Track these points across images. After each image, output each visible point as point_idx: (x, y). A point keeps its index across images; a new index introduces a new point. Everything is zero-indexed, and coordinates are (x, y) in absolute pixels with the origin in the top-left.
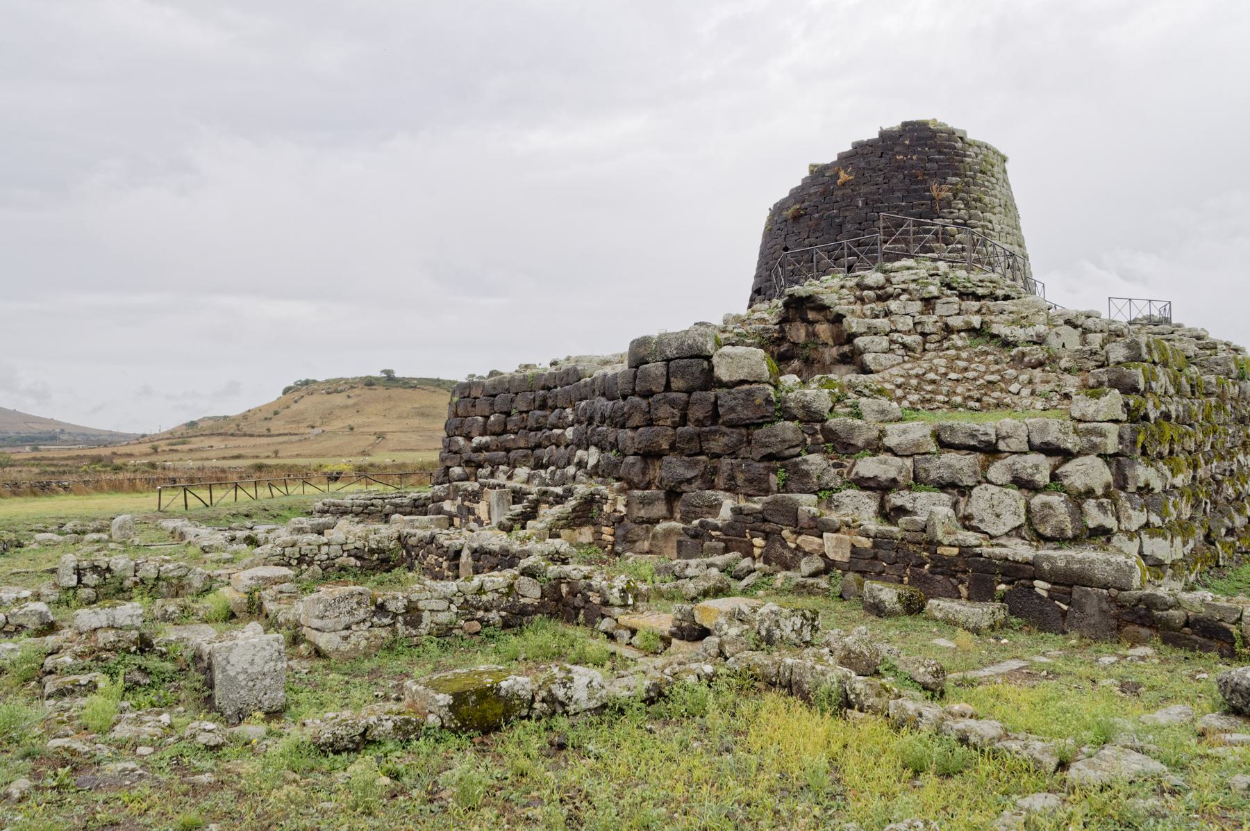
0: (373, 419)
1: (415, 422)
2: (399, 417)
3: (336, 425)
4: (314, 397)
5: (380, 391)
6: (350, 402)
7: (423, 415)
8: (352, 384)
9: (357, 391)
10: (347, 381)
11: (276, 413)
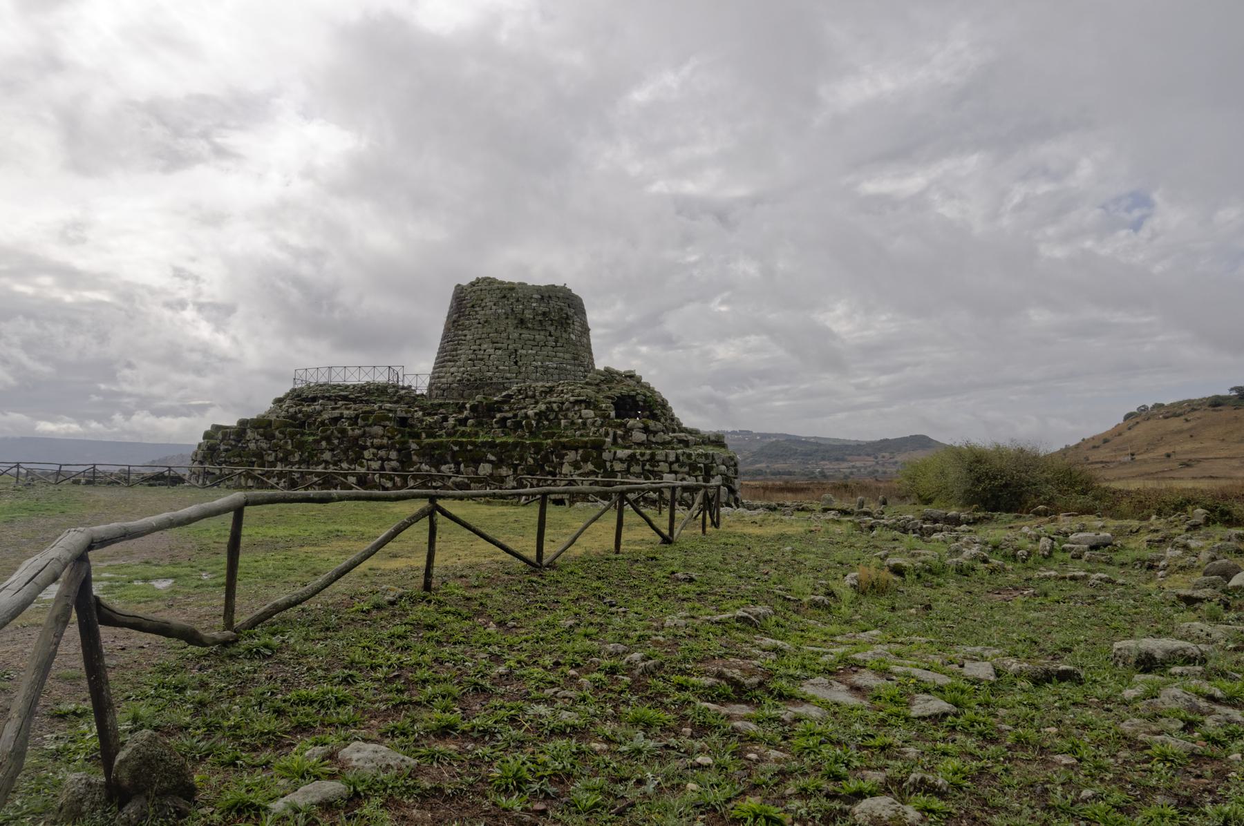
0: (1208, 444)
4: (1148, 423)
5: (1226, 412)
8: (1192, 406)
9: (1197, 414)
10: (1190, 402)
11: (1106, 441)
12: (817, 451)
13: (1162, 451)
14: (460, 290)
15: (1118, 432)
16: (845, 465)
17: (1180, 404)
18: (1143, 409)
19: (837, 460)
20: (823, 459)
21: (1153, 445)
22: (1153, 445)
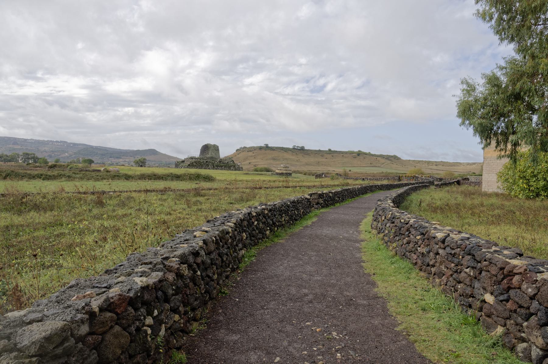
1: (272, 161)
3: (248, 162)
5: (263, 151)
9: (256, 151)
10: (254, 147)
13: (248, 162)
15: (235, 155)
16: (121, 160)
17: (251, 147)
18: (241, 148)
19: (117, 158)
20: (111, 157)
21: (245, 159)
22: (245, 159)
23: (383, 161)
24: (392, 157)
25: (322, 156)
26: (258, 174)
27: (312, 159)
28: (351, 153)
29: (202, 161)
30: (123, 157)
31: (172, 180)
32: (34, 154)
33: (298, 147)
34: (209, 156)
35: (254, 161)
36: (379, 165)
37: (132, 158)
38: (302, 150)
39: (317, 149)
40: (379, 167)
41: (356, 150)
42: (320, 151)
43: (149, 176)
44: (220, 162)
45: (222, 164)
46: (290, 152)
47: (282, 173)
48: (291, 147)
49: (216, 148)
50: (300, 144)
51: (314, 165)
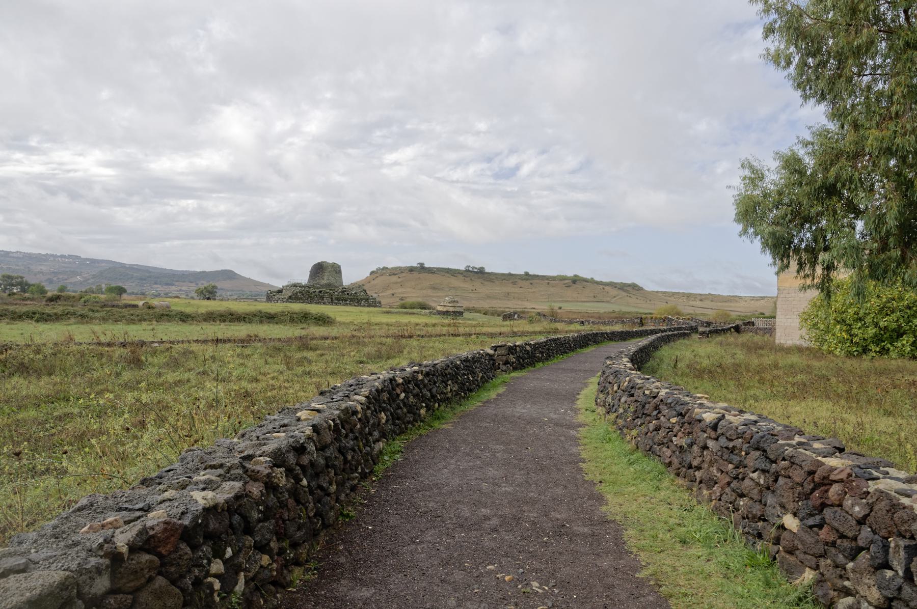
1: (430, 292)
2: (422, 289)
3: (390, 292)
5: (415, 274)
6: (399, 280)
7: (434, 288)
9: (404, 275)
12: (150, 277)
13: (390, 292)
14: (319, 263)
15: (368, 280)
16: (174, 288)
17: (396, 268)
18: (379, 269)
19: (167, 284)
20: (156, 283)
21: (386, 287)
22: (386, 287)
23: (614, 292)
24: (629, 285)
25: (514, 283)
26: (407, 313)
27: (497, 289)
28: (562, 278)
29: (312, 290)
30: (177, 283)
31: (261, 322)
32: (22, 278)
33: (473, 268)
34: (324, 282)
35: (400, 290)
36: (608, 299)
37: (193, 285)
38: (480, 273)
39: (506, 272)
40: (608, 302)
41: (570, 274)
42: (510, 275)
43: (221, 316)
44: (343, 292)
45: (347, 296)
46: (460, 276)
47: (447, 312)
48: (462, 268)
49: (336, 270)
50: (477, 264)
51: (500, 299)
